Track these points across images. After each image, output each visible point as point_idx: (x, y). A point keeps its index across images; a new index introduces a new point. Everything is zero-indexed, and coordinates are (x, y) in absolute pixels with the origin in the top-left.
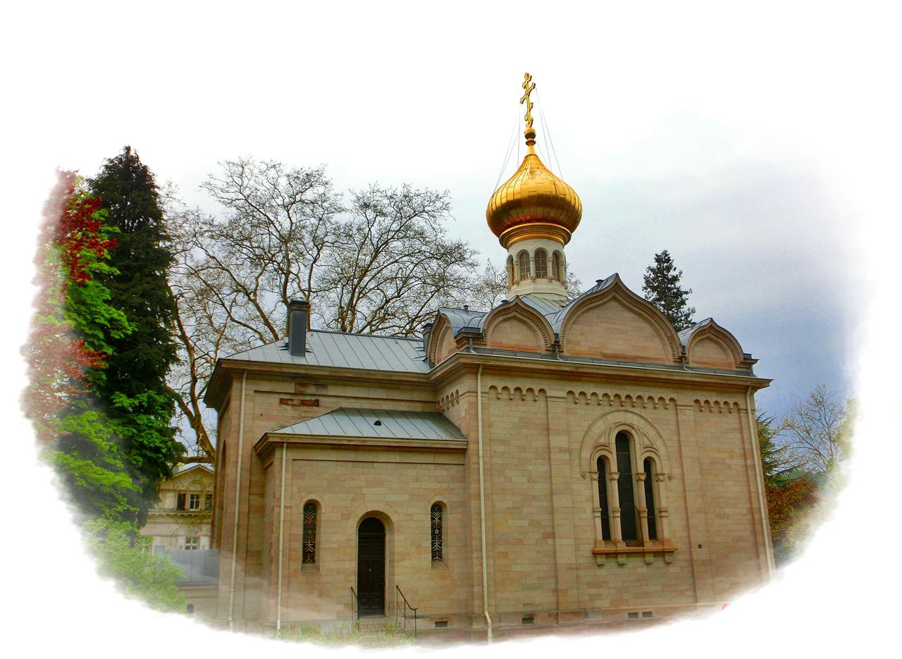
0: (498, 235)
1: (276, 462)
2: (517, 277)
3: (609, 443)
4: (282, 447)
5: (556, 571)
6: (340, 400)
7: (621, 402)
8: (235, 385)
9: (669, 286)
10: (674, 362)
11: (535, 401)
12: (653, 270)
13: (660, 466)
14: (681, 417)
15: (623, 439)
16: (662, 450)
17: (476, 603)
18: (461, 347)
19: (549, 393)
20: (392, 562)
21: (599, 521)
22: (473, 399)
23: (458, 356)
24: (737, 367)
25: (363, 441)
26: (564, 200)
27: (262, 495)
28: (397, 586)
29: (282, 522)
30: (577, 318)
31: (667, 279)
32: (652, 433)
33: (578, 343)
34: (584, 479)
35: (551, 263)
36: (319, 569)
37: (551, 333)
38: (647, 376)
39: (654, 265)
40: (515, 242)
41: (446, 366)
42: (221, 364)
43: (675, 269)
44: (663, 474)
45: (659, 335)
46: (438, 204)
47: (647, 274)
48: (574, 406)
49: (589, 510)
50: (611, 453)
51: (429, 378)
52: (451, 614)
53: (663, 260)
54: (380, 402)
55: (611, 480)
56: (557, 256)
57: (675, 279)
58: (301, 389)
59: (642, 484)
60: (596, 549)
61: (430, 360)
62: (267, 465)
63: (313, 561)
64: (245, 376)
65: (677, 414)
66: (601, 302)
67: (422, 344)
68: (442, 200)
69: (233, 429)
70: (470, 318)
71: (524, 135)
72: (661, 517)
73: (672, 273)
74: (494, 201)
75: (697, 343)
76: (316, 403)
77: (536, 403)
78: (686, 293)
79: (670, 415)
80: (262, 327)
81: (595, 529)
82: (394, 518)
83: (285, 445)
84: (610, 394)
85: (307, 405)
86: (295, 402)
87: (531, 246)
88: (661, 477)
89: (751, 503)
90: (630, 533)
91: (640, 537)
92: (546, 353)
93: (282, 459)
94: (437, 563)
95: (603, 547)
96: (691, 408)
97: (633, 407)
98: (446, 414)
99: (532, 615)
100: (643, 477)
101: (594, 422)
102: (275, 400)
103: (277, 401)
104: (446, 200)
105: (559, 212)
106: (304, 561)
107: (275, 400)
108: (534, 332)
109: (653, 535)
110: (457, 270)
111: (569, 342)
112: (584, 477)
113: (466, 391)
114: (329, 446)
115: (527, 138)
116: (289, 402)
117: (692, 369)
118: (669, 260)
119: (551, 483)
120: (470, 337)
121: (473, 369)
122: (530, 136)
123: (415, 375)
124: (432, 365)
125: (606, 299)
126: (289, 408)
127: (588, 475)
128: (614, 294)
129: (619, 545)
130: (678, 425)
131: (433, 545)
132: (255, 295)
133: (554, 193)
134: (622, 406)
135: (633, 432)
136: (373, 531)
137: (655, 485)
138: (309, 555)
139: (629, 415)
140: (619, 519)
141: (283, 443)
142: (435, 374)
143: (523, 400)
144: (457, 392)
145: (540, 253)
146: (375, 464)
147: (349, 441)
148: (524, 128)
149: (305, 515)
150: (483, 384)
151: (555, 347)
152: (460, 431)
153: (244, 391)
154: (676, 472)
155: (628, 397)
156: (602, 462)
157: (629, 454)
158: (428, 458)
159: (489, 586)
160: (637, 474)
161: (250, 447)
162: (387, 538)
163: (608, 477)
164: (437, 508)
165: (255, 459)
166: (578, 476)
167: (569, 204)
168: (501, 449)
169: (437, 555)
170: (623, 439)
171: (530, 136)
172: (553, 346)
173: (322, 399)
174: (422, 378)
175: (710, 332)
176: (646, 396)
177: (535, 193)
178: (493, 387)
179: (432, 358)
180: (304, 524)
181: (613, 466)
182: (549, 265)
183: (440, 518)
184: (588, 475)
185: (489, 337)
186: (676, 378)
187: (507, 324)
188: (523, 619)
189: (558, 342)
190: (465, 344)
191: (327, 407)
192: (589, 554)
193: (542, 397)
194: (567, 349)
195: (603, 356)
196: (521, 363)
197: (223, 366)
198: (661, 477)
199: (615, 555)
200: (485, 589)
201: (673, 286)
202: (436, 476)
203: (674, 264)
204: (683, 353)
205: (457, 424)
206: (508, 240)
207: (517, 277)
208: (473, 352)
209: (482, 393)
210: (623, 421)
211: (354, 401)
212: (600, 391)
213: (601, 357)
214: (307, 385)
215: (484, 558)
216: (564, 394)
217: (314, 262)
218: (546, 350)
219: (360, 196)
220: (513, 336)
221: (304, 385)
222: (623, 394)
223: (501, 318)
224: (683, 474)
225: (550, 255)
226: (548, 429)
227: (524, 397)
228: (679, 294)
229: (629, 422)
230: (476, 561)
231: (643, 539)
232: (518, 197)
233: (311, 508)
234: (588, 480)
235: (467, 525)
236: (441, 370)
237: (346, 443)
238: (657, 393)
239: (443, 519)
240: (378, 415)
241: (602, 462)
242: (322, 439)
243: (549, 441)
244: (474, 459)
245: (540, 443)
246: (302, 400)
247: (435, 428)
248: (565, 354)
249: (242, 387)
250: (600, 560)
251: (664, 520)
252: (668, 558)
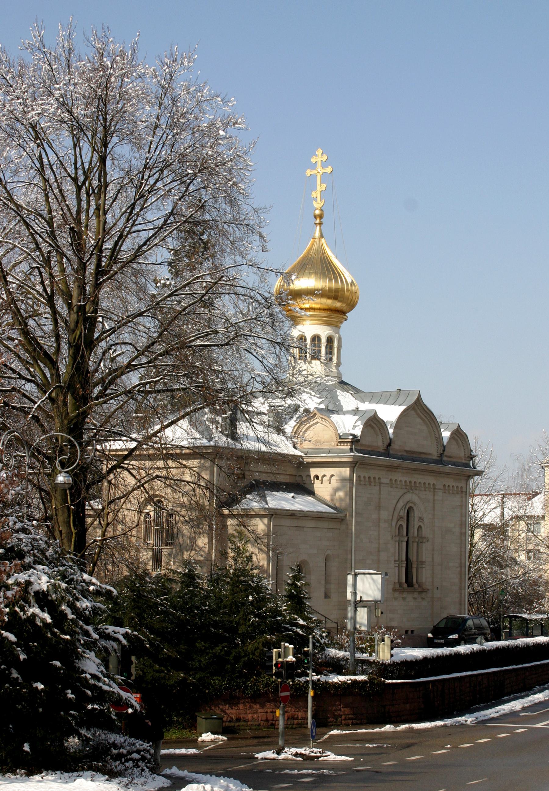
13: (426, 532)
59: (415, 544)
89: (461, 559)
130: (434, 503)
135: (415, 508)
216: (387, 481)
226: (379, 507)
252: (423, 595)
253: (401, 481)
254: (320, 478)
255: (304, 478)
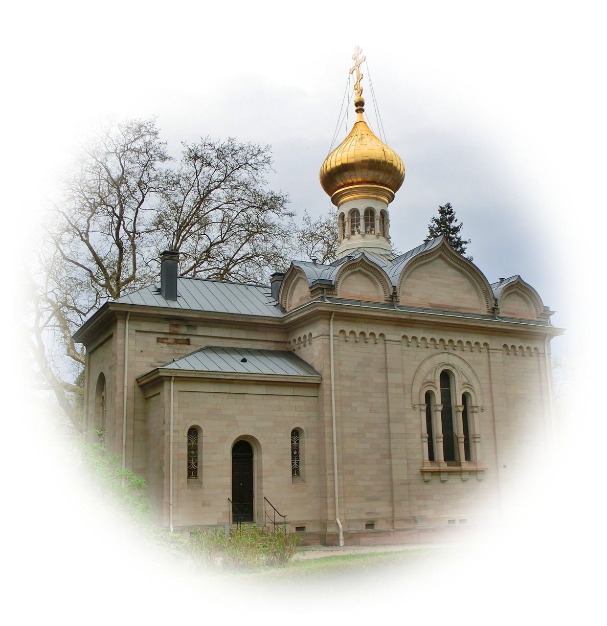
0: (330, 194)
1: (166, 393)
2: (346, 234)
3: (435, 380)
4: (170, 381)
5: (392, 485)
6: (207, 339)
7: (445, 346)
8: (120, 325)
9: (451, 235)
10: (488, 312)
11: (376, 343)
12: (437, 221)
13: (476, 400)
14: (492, 359)
15: (446, 377)
16: (476, 387)
17: (330, 511)
18: (315, 296)
19: (388, 337)
20: (260, 477)
21: (426, 445)
22: (326, 341)
23: (316, 304)
24: (537, 318)
25: (236, 376)
26: (391, 165)
27: (145, 421)
28: (265, 498)
29: (171, 444)
30: (411, 272)
31: (449, 229)
32: (469, 372)
33: (411, 294)
34: (415, 410)
35: (378, 221)
36: (202, 484)
37: (390, 286)
38: (467, 324)
39: (438, 216)
40: (347, 201)
41: (300, 313)
42: (109, 306)
43: (456, 221)
44: (477, 407)
45: (477, 290)
46: (260, 158)
47: (432, 225)
48: (407, 348)
49: (418, 436)
50: (437, 389)
51: (283, 321)
52: (308, 521)
53: (446, 212)
54: (241, 342)
55: (435, 411)
56: (384, 214)
57: (456, 230)
58: (176, 329)
59: (460, 415)
60: (425, 468)
61: (281, 305)
62: (150, 395)
63: (196, 477)
64: (128, 317)
65: (489, 357)
66: (428, 260)
67: (270, 291)
68: (263, 154)
69: (119, 364)
70: (321, 270)
71: (354, 103)
72: (475, 442)
73: (453, 224)
74: (329, 163)
75: (506, 296)
76: (188, 342)
77: (377, 345)
78: (466, 243)
79: (482, 357)
80: (94, 267)
81: (423, 451)
82: (261, 441)
83: (173, 378)
84: (436, 338)
85: (179, 344)
86: (170, 341)
87: (361, 206)
88: (476, 409)
90: (450, 455)
91: (458, 459)
92: (386, 302)
93: (170, 390)
94: (297, 479)
95: (429, 466)
96: (501, 352)
97: (454, 350)
98: (296, 353)
99: (372, 521)
100: (461, 409)
101: (423, 362)
102: (152, 339)
103: (155, 340)
104: (268, 154)
105: (387, 176)
106: (189, 477)
107: (152, 339)
108: (375, 284)
109: (468, 457)
110: (271, 217)
111: (404, 293)
112: (414, 408)
113: (321, 334)
114: (209, 380)
115: (357, 107)
116: (165, 341)
117: (502, 318)
118: (451, 212)
119: (388, 413)
120: (324, 287)
121: (327, 316)
122: (360, 104)
123: (271, 319)
124: (283, 310)
125: (434, 257)
126: (165, 345)
127: (417, 406)
128: (441, 252)
129: (441, 464)
131: (293, 464)
132: (87, 235)
133: (383, 159)
134: (445, 349)
135: (454, 371)
136: (244, 452)
137: (470, 415)
138: (193, 472)
139: (451, 357)
140: (442, 444)
141: (171, 377)
142: (288, 318)
143: (366, 342)
144: (310, 334)
145: (370, 212)
146: (246, 395)
147: (225, 375)
148: (355, 98)
149: (188, 438)
150: (334, 328)
151: (393, 298)
152: (313, 368)
153: (127, 331)
154: (488, 404)
155: (451, 341)
156: (429, 396)
157: (450, 390)
158: (290, 391)
159: (339, 497)
160: (457, 406)
161: (133, 381)
162: (255, 458)
163: (433, 409)
164: (296, 433)
165: (138, 390)
166: (410, 407)
167: (395, 168)
168: (348, 384)
169: (296, 471)
170: (446, 377)
171: (360, 104)
172: (392, 297)
173: (192, 339)
174: (276, 321)
175: (517, 287)
176: (464, 340)
177: (367, 158)
178: (342, 331)
179: (283, 304)
180: (188, 446)
181: (438, 399)
182: (376, 221)
183: (298, 442)
184: (417, 406)
185: (339, 288)
186: (490, 326)
187: (353, 277)
188: (366, 525)
189: (396, 293)
190: (320, 293)
191: (196, 346)
192: (418, 472)
193: (381, 339)
194: (403, 300)
195: (431, 306)
196: (366, 311)
197: (110, 308)
198: (476, 409)
199: (439, 473)
200: (337, 500)
201: (454, 236)
202: (295, 406)
203: (456, 217)
204: (495, 305)
205: (309, 362)
206: (338, 201)
207: (348, 232)
208: (327, 301)
209: (334, 336)
210: (446, 361)
211: (219, 340)
212: (429, 336)
213: (430, 308)
214: (181, 325)
215: (336, 474)
217: (139, 207)
218: (386, 300)
219: (192, 148)
220: (357, 289)
221: (177, 326)
222: (464, 340)
223: (349, 272)
224: (493, 407)
225: (378, 214)
226: (386, 368)
227: (367, 340)
228: (459, 243)
229: (451, 362)
230: (329, 478)
231: (460, 460)
232: (352, 161)
233: (194, 432)
234: (417, 411)
235: (321, 445)
236: (295, 315)
237: (223, 377)
238: (473, 339)
239: (300, 442)
240: (245, 353)
241: (429, 396)
242: (203, 374)
243: (387, 378)
244: (327, 393)
245: (379, 380)
246: (176, 339)
247: (293, 366)
248: (401, 304)
249: (125, 327)
250: (427, 477)
251: (478, 445)
252: (479, 476)
253: (423, 338)
254: (302, 341)
255: (292, 344)
